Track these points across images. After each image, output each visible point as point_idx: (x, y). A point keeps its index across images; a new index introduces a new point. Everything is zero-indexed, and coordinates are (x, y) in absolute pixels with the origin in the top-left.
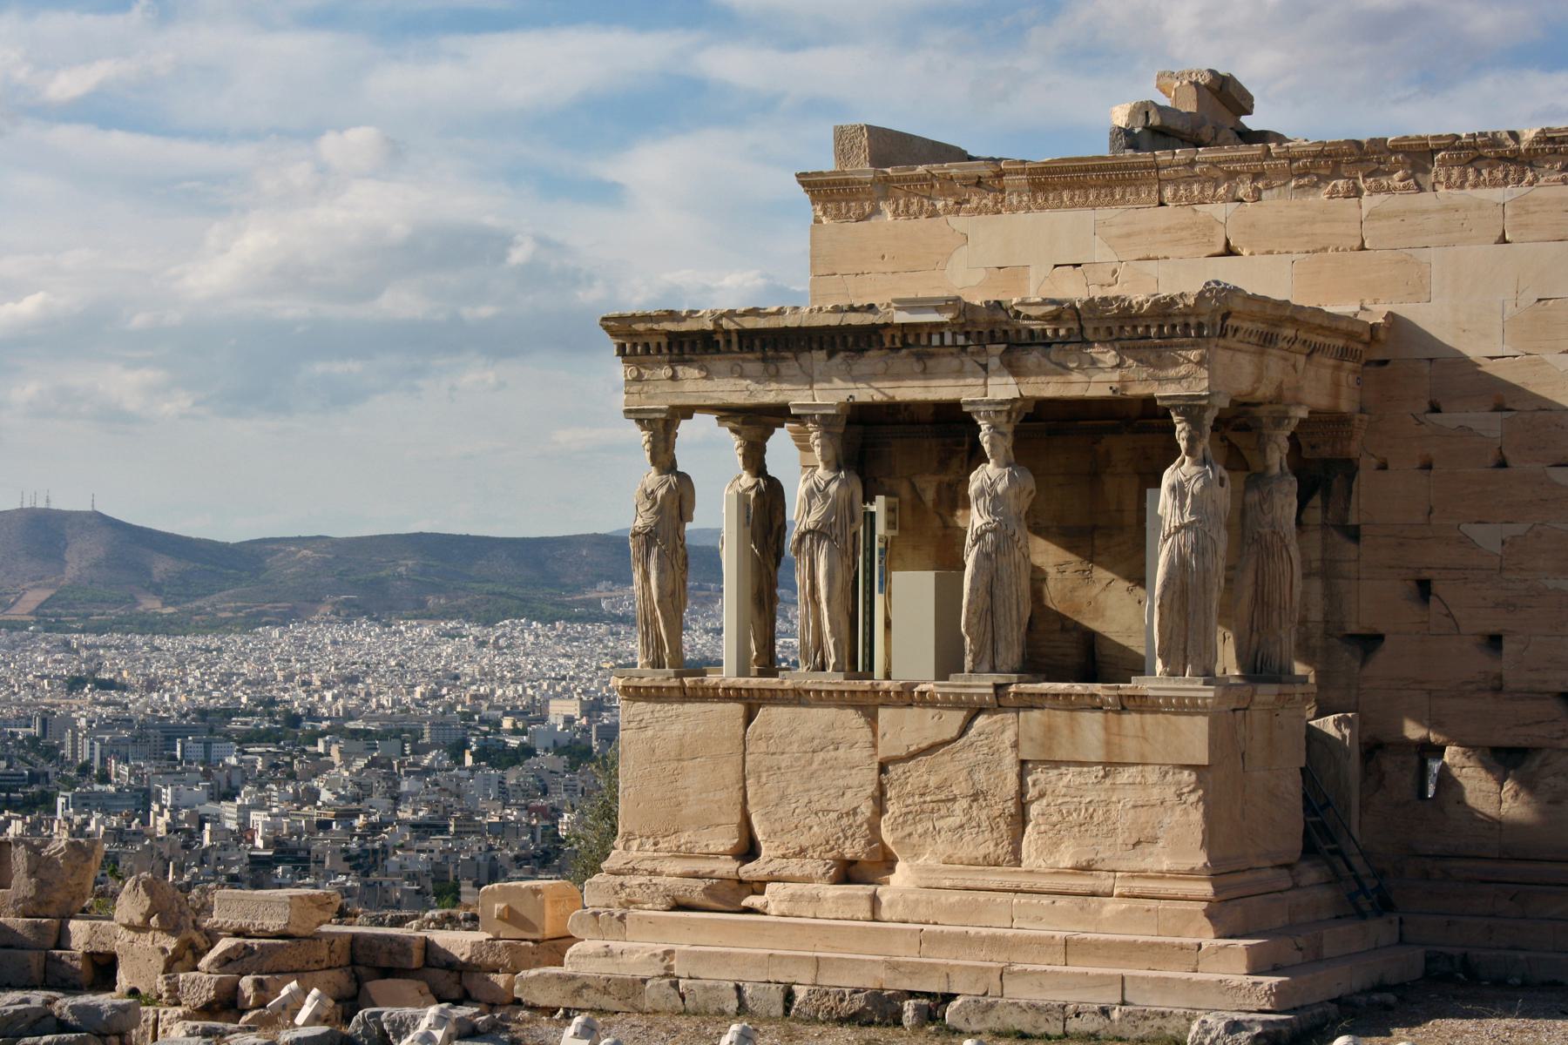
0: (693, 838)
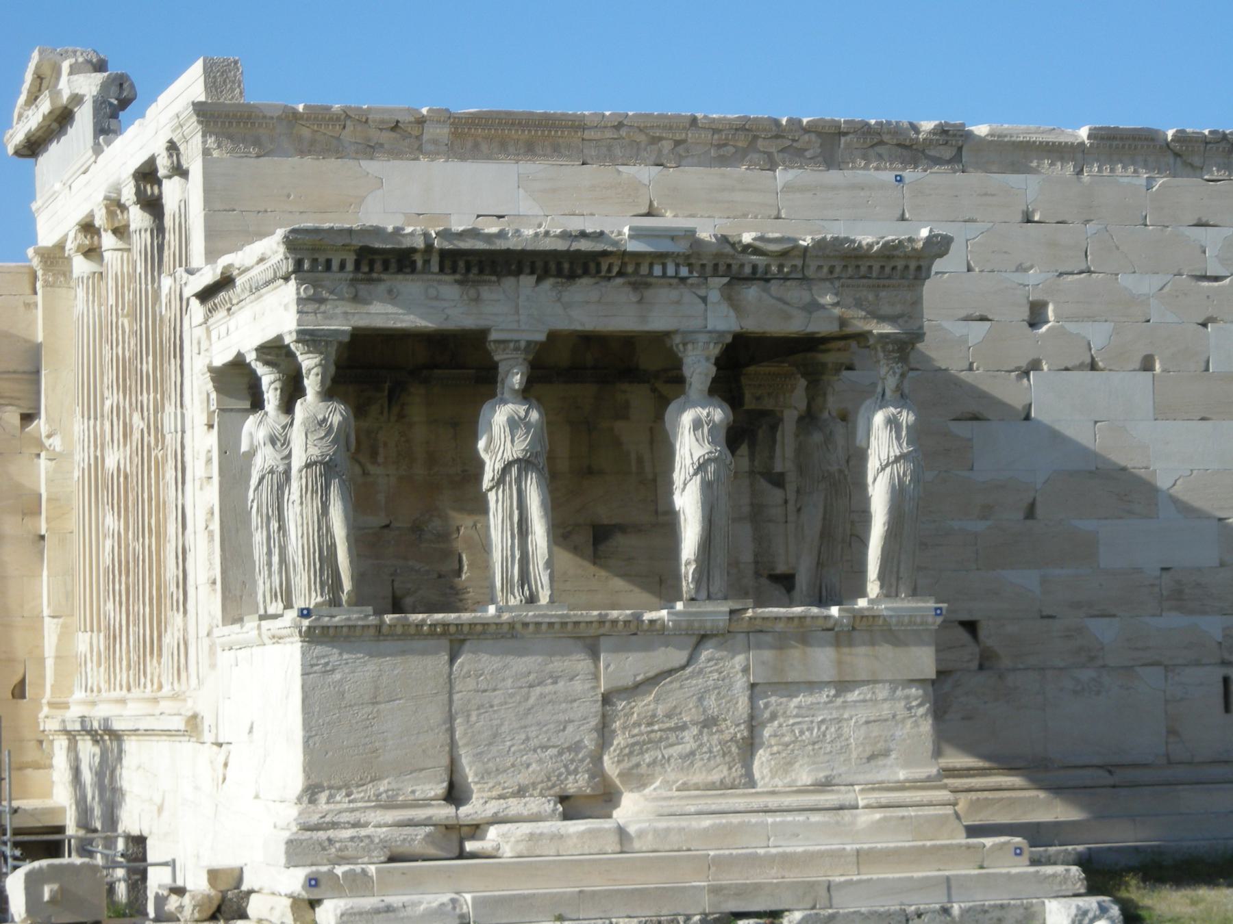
0: (394, 786)
